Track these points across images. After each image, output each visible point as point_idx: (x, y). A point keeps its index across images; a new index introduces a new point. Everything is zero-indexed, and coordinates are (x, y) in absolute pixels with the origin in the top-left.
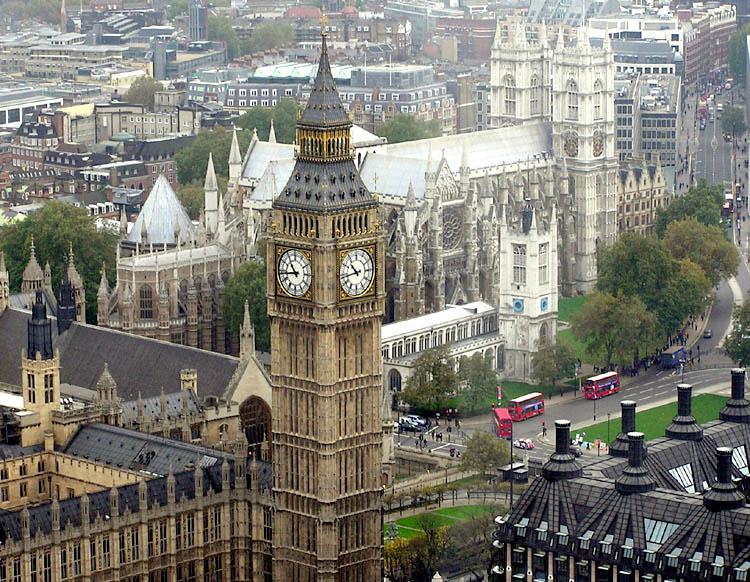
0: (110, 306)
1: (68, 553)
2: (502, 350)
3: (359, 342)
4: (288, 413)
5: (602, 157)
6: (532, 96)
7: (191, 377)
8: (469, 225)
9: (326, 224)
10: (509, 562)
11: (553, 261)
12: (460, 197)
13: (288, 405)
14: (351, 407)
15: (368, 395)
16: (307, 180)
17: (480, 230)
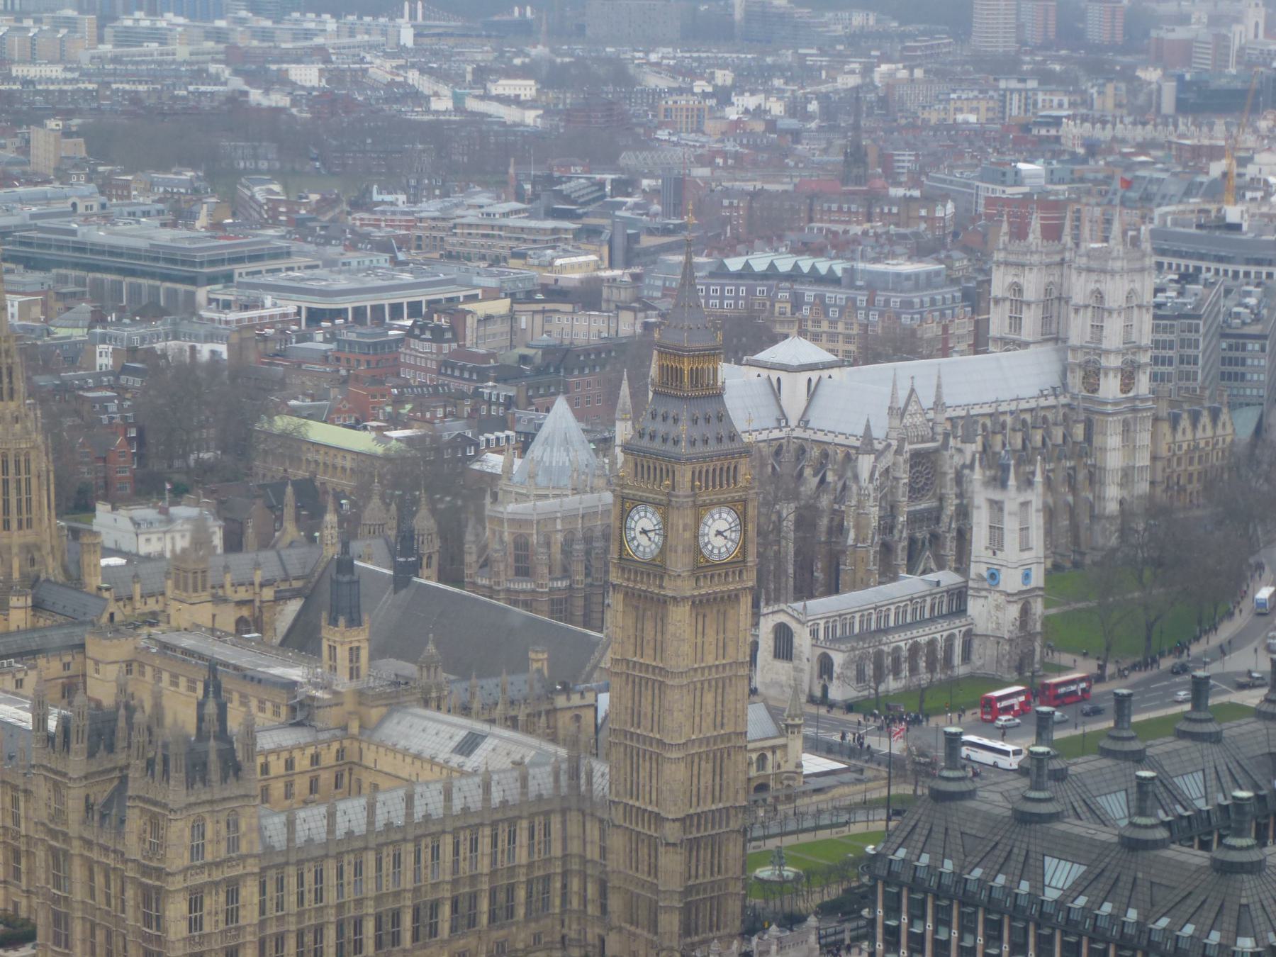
0: (479, 557)
1: (346, 867)
2: (969, 637)
3: (721, 618)
4: (630, 705)
5: (1131, 394)
6: (1045, 308)
7: (540, 656)
8: (945, 474)
9: (684, 475)
10: (880, 903)
11: (1037, 522)
12: (933, 440)
13: (630, 695)
14: (709, 698)
15: (730, 685)
16: (665, 418)
17: (959, 479)
